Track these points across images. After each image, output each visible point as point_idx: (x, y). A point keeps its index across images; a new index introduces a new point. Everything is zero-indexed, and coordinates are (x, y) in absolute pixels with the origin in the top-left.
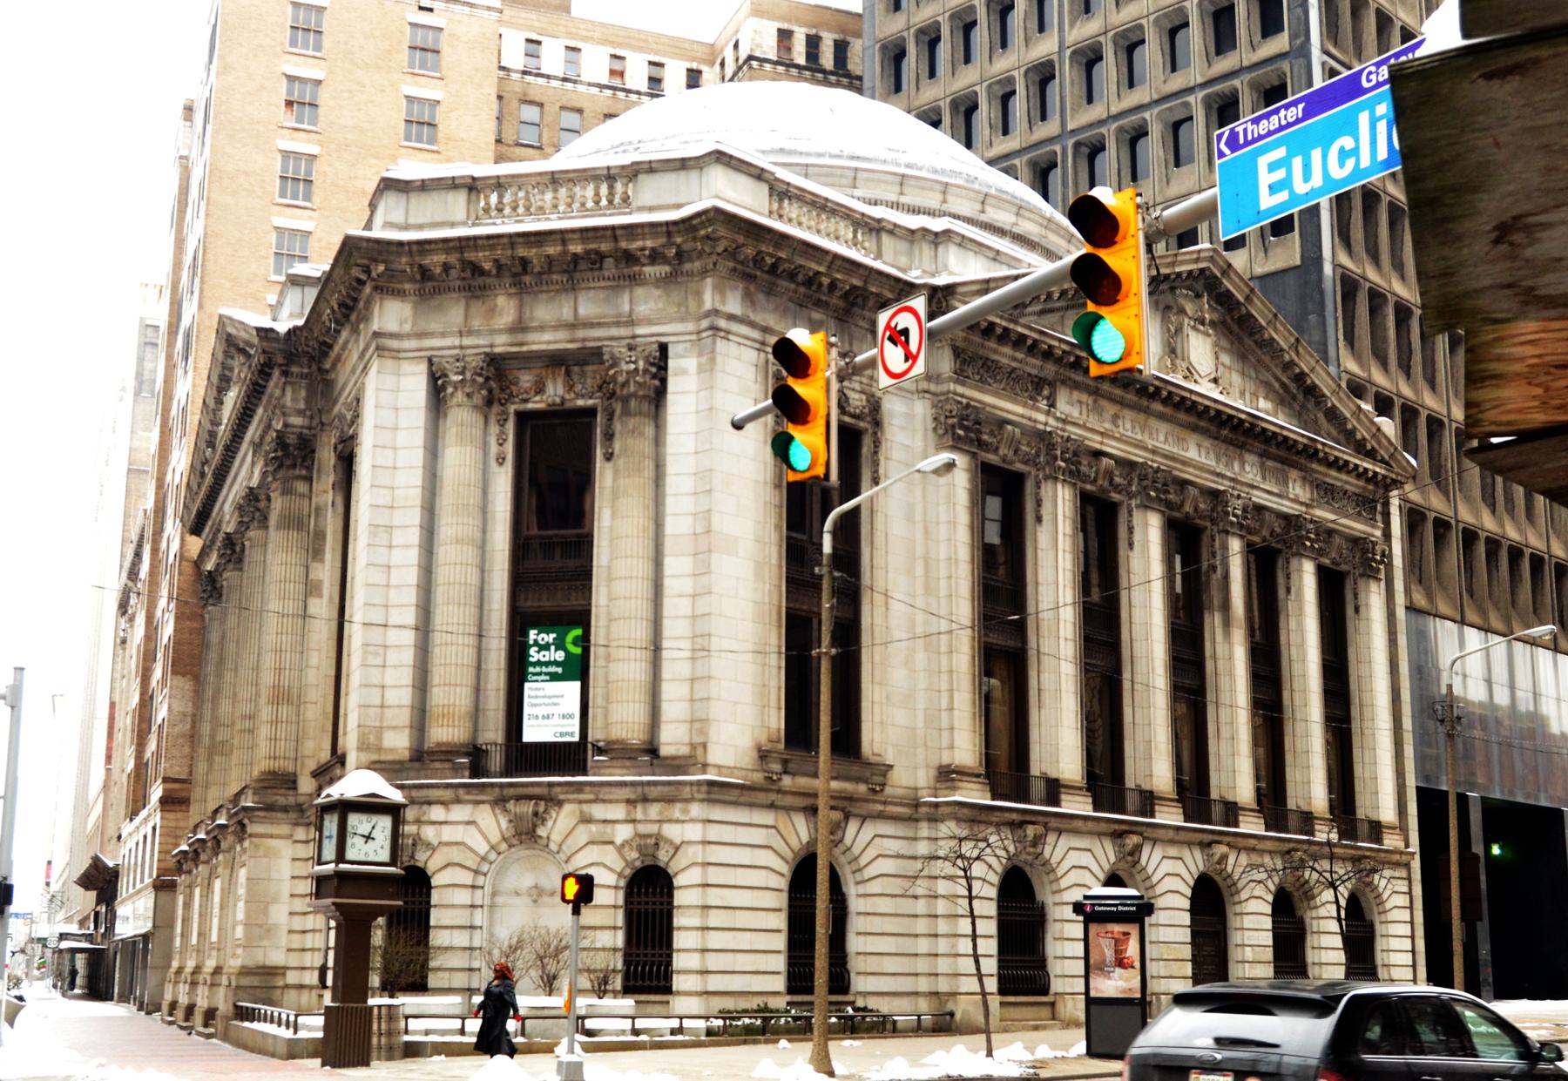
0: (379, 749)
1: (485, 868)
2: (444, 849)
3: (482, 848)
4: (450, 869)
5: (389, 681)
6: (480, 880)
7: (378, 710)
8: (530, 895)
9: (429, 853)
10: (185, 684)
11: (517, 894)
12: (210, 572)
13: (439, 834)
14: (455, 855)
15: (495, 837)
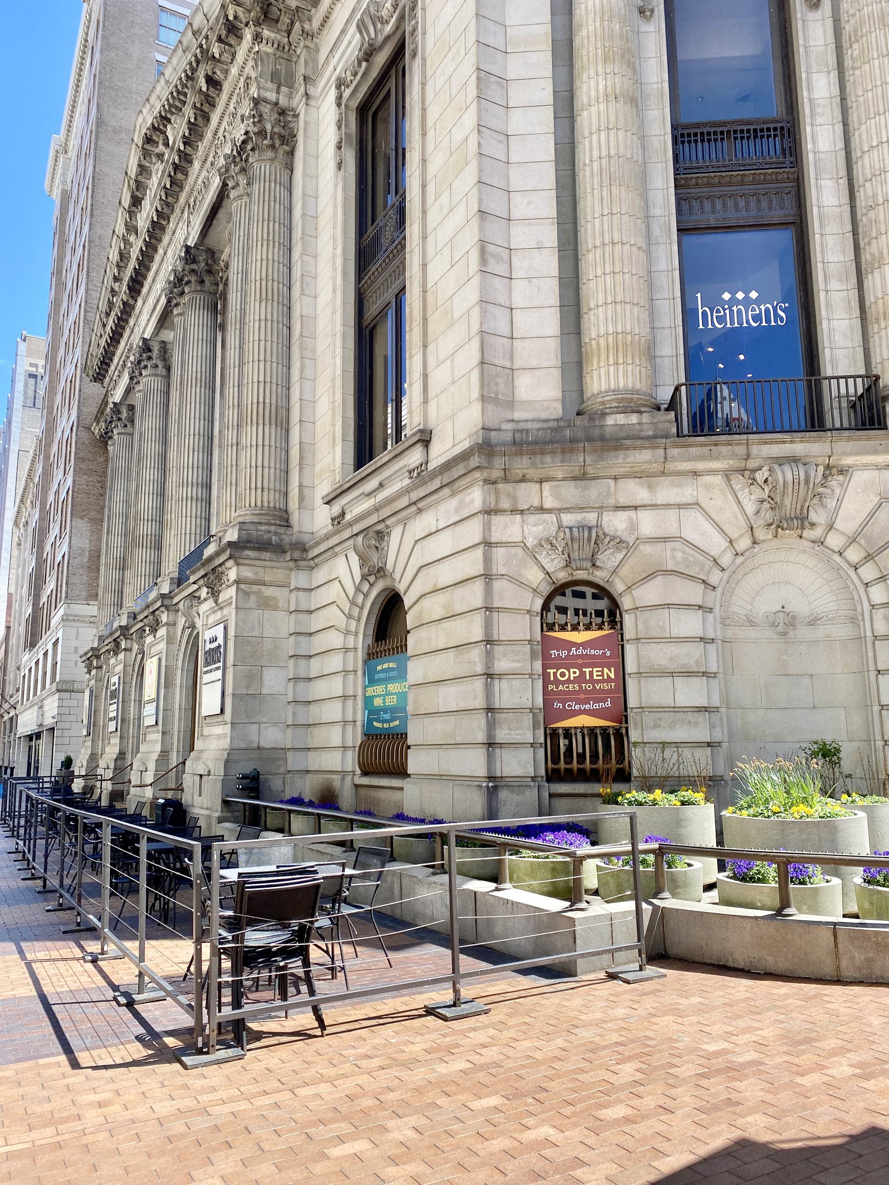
0: (511, 404)
1: (715, 578)
2: (646, 549)
3: (716, 544)
4: (659, 580)
5: (518, 300)
6: (712, 599)
7: (506, 341)
8: (774, 625)
9: (619, 556)
10: (83, 526)
11: (752, 623)
12: (115, 404)
13: (633, 526)
14: (671, 556)
15: (737, 528)
